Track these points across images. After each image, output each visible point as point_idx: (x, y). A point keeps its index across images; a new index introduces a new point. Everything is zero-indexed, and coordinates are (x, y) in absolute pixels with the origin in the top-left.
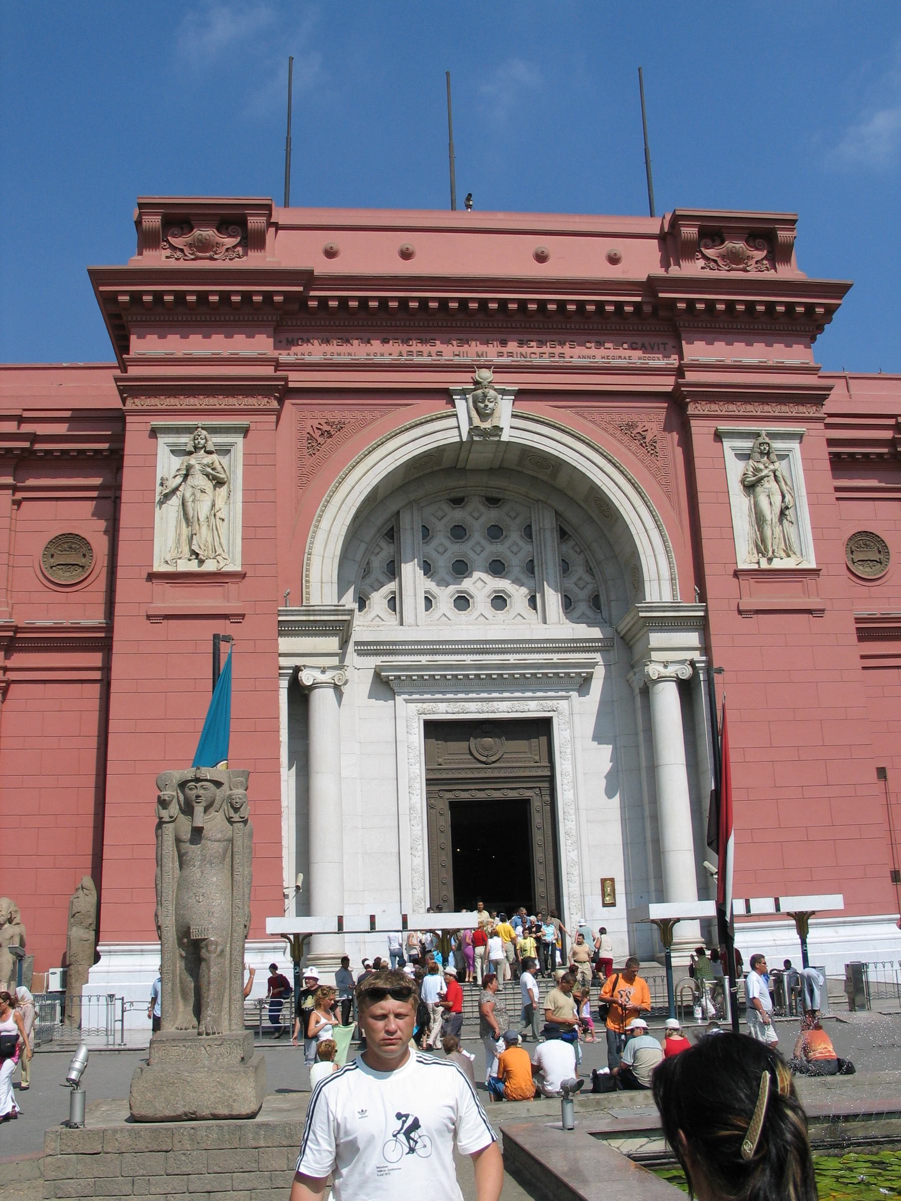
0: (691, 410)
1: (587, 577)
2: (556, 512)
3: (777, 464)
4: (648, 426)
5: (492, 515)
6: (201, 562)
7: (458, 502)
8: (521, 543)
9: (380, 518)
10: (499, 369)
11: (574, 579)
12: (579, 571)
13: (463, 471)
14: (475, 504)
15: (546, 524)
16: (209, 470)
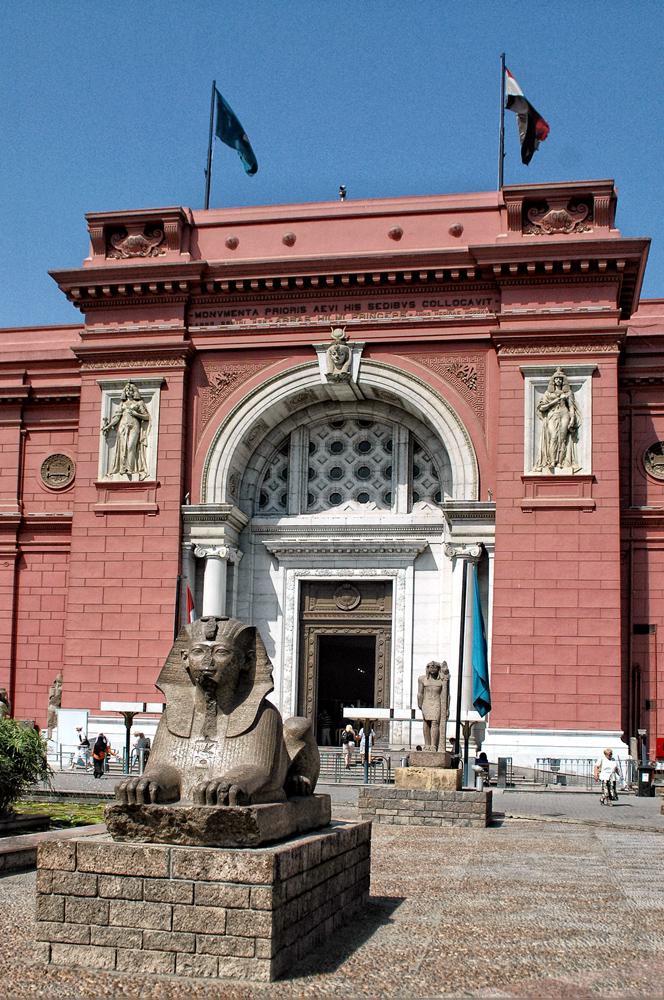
0: (500, 353)
1: (432, 479)
2: (410, 431)
3: (569, 393)
4: (470, 366)
5: (364, 434)
6: (130, 476)
7: (337, 425)
8: (384, 454)
9: (275, 440)
10: (350, 328)
11: (422, 480)
12: (427, 475)
13: (337, 403)
14: (351, 426)
15: (401, 438)
16: (135, 413)
